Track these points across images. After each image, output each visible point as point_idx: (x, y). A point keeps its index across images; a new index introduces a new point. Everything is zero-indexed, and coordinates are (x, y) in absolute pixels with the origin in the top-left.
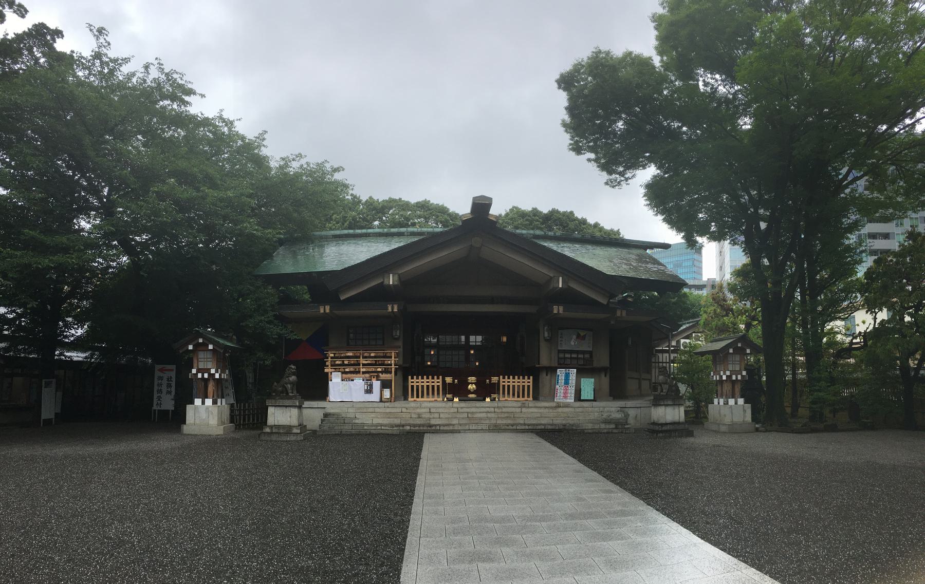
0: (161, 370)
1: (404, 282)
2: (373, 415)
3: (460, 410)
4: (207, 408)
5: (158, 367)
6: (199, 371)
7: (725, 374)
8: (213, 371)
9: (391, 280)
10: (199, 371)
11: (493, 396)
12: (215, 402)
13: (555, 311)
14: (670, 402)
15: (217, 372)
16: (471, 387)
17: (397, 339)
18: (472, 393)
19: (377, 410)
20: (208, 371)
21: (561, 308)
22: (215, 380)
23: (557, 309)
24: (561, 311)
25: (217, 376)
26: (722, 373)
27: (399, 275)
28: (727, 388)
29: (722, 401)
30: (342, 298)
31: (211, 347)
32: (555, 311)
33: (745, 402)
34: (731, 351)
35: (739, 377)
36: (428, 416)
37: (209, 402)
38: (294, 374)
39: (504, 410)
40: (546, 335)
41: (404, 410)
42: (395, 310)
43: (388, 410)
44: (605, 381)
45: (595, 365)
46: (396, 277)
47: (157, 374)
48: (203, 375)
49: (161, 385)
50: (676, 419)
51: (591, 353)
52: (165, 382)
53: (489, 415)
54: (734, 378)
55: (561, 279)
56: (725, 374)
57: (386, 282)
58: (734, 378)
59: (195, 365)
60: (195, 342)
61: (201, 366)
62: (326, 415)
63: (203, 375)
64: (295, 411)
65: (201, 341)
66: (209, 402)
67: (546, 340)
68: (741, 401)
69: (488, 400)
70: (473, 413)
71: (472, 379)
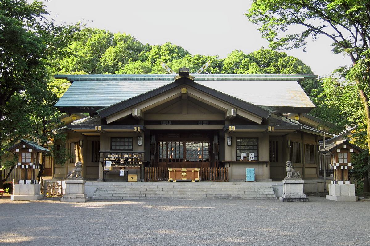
1: (146, 113)
2: (125, 189)
3: (175, 187)
7: (335, 165)
8: (31, 164)
9: (136, 113)
10: (22, 164)
15: (34, 164)
19: (127, 186)
21: (234, 128)
24: (234, 129)
25: (34, 167)
27: (141, 110)
28: (336, 174)
30: (108, 122)
31: (30, 150)
32: (230, 129)
33: (351, 183)
34: (339, 151)
35: (346, 167)
36: (156, 189)
39: (201, 187)
40: (228, 143)
42: (139, 130)
53: (191, 189)
54: (342, 167)
55: (232, 110)
56: (335, 165)
57: (133, 114)
58: (342, 167)
59: (20, 160)
62: (97, 189)
65: (24, 146)
67: (229, 146)
68: (347, 182)
69: (193, 181)
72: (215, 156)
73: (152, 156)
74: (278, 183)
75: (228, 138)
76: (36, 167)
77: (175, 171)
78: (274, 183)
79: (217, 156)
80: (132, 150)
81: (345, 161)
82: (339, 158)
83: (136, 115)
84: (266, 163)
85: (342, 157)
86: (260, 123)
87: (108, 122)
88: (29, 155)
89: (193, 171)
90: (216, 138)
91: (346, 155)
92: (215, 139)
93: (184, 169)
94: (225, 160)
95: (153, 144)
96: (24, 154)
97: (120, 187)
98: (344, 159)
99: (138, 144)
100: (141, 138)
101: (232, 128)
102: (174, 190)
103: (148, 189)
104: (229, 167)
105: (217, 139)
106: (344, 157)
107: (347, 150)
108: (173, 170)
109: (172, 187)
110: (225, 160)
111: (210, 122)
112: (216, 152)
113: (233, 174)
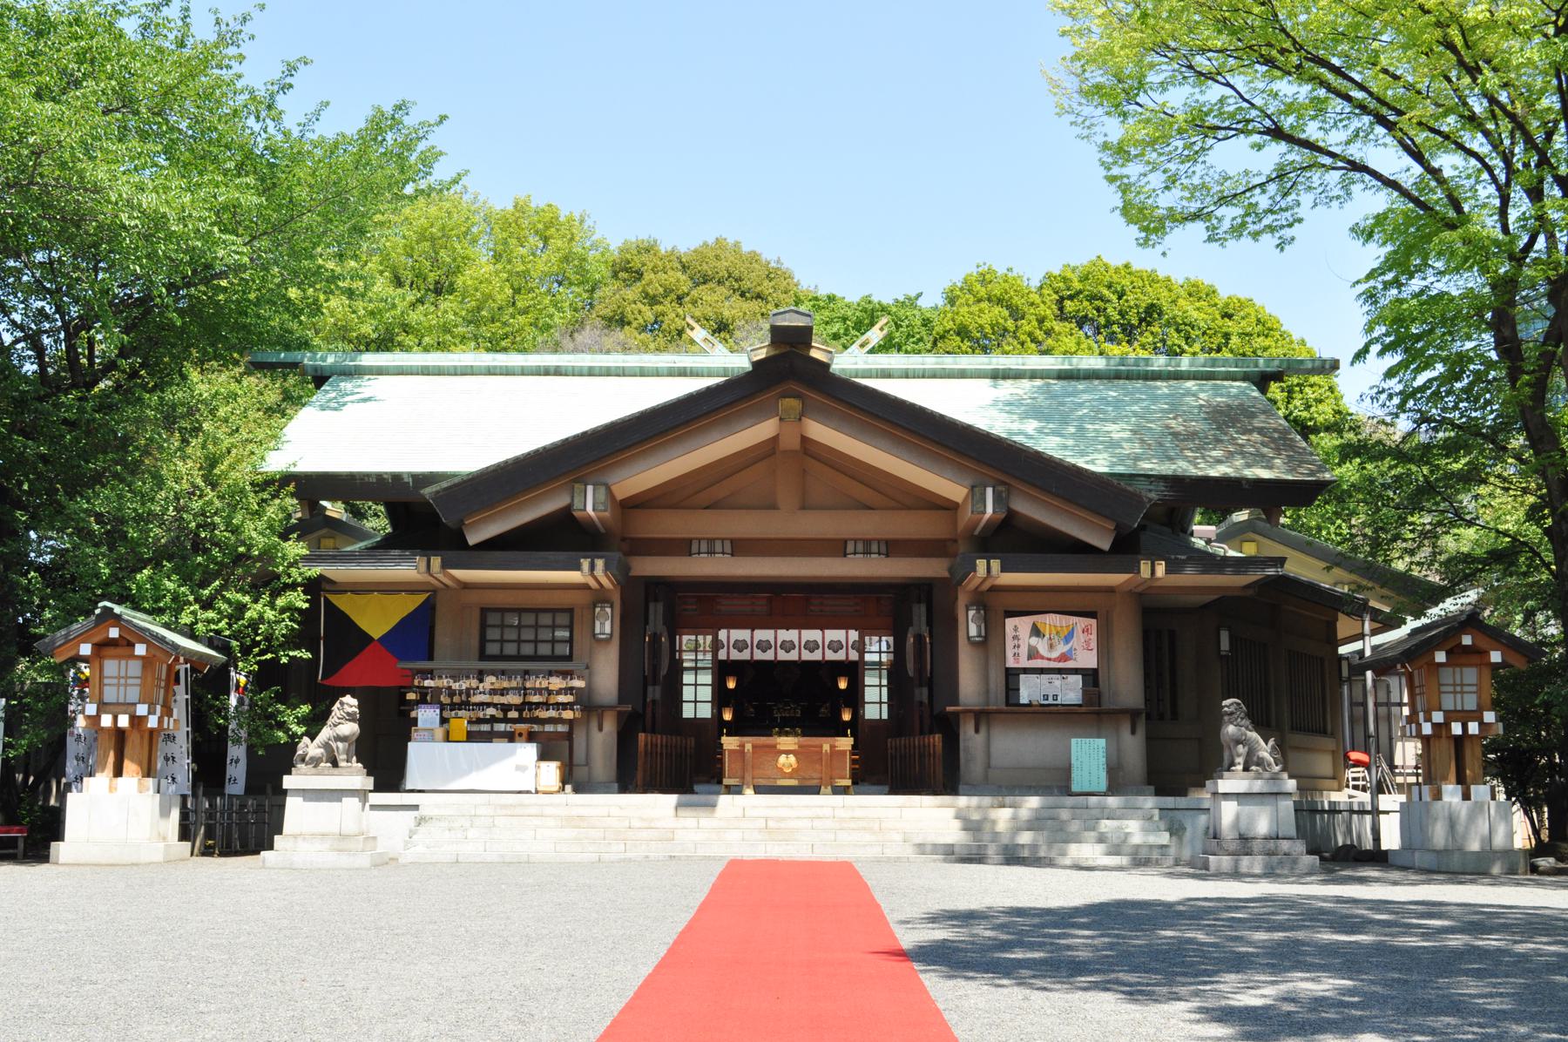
8: (142, 710)
10: (103, 707)
18: (790, 776)
19: (548, 811)
20: (128, 707)
25: (153, 722)
31: (140, 650)
34: (1440, 657)
35: (1473, 728)
40: (973, 631)
54: (1457, 729)
56: (1428, 719)
58: (1457, 729)
65: (114, 633)
72: (917, 691)
73: (650, 689)
74: (1181, 802)
75: (971, 613)
77: (748, 747)
78: (1169, 801)
79: (925, 691)
80: (569, 658)
81: (1470, 703)
82: (1443, 689)
84: (1133, 715)
85: (1455, 685)
86: (1105, 544)
87: (473, 539)
88: (135, 668)
89: (826, 747)
90: (920, 611)
91: (1470, 675)
92: (915, 618)
93: (787, 742)
94: (957, 704)
95: (655, 638)
96: (111, 667)
98: (1462, 693)
99: (594, 635)
100: (608, 610)
101: (988, 571)
103: (636, 823)
104: (977, 731)
105: (924, 619)
106: (1462, 685)
107: (1478, 653)
108: (742, 746)
109: (740, 813)
110: (957, 704)
111: (893, 548)
112: (920, 669)
113: (993, 763)
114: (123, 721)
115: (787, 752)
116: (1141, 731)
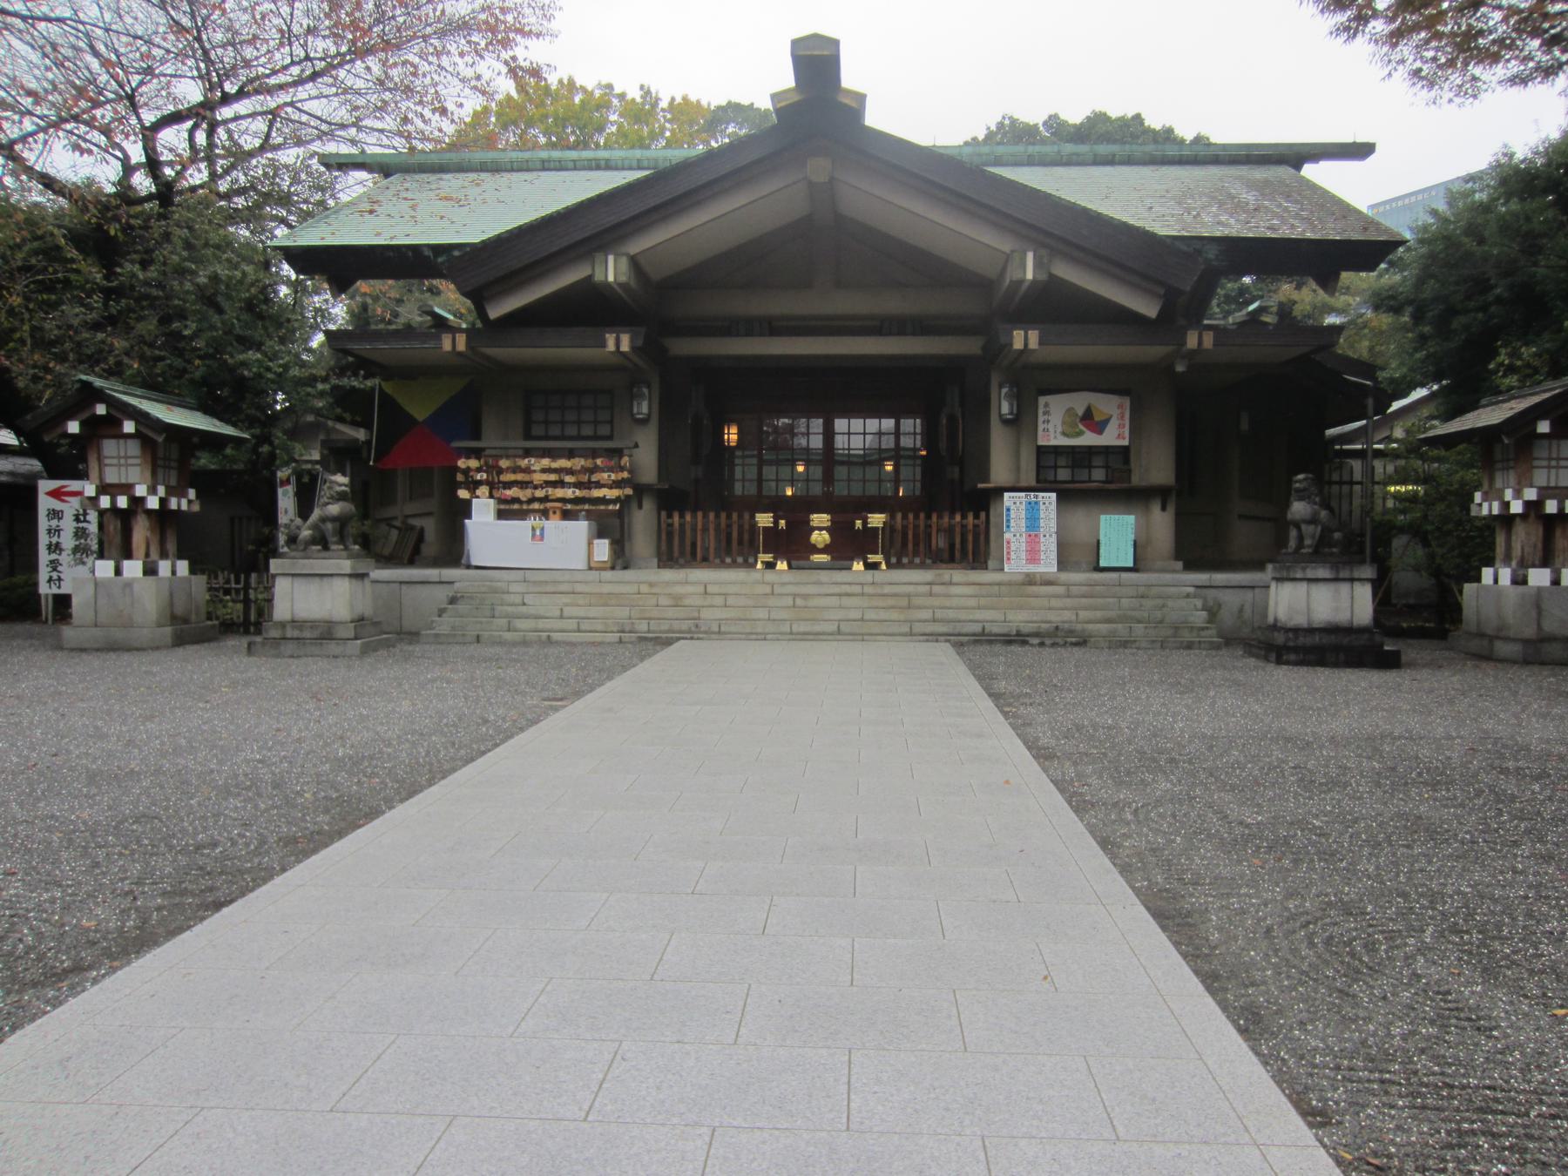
0: (56, 494)
4: (129, 584)
5: (45, 485)
6: (103, 489)
8: (141, 491)
9: (612, 270)
11: (872, 558)
12: (150, 570)
13: (1018, 344)
14: (1323, 572)
15: (152, 490)
16: (820, 538)
17: (644, 422)
20: (127, 489)
21: (1034, 336)
22: (150, 512)
23: (1023, 339)
26: (1508, 494)
27: (634, 262)
28: (1524, 538)
29: (1505, 575)
31: (129, 427)
36: (698, 601)
37: (133, 568)
38: (341, 497)
39: (887, 590)
40: (1005, 408)
41: (645, 589)
42: (625, 347)
43: (606, 589)
44: (1162, 521)
45: (1136, 480)
46: (624, 261)
47: (45, 503)
48: (113, 502)
49: (58, 531)
50: (1342, 617)
51: (1124, 452)
52: (68, 525)
53: (846, 601)
57: (599, 277)
60: (85, 415)
61: (112, 477)
63: (113, 502)
64: (343, 586)
66: (133, 568)
67: (1006, 422)
70: (805, 597)
71: (820, 519)
76: (163, 501)
83: (611, 278)
97: (550, 588)
102: (772, 602)
114: (122, 502)
115: (820, 529)
116: (1171, 509)
